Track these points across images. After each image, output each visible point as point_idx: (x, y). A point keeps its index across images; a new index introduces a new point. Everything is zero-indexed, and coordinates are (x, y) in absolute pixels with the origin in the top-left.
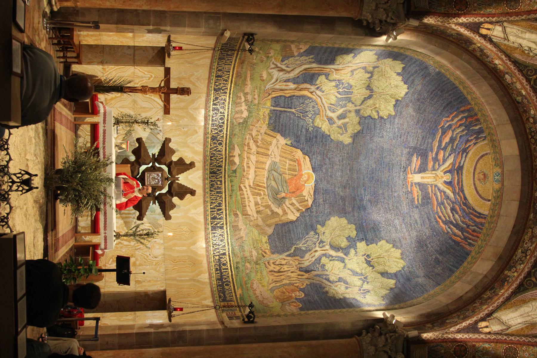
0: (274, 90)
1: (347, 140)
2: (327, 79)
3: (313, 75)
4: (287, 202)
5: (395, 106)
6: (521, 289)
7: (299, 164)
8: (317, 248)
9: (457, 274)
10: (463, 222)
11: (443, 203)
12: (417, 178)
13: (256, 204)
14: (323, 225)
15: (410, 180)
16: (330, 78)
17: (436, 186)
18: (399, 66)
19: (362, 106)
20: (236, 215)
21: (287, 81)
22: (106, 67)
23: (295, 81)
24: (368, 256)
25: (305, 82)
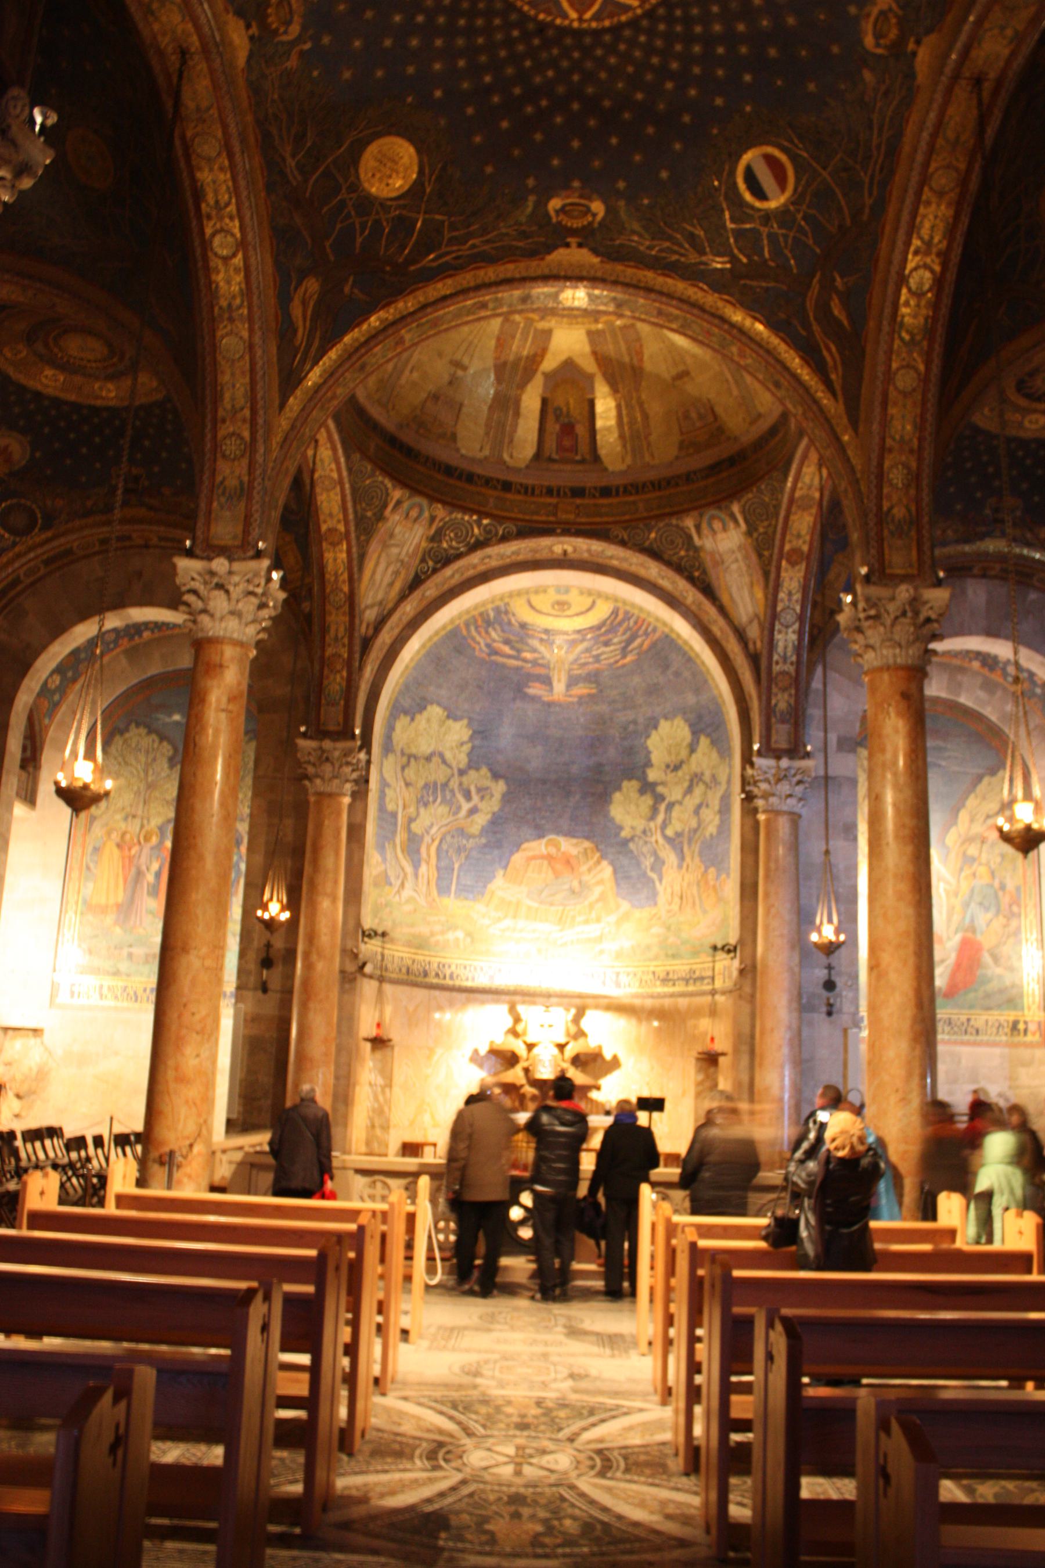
0: (429, 893)
1: (499, 788)
2: (415, 820)
3: (409, 839)
4: (586, 878)
5: (456, 719)
6: (708, 591)
7: (534, 858)
8: (653, 839)
9: (692, 655)
10: (624, 634)
11: (598, 656)
12: (559, 687)
13: (586, 922)
14: (621, 828)
15: (562, 698)
16: (414, 815)
17: (572, 663)
18: (402, 722)
19: (454, 764)
20: (602, 952)
21: (416, 875)
22: (392, 1124)
23: (416, 866)
24: (668, 766)
25: (418, 851)
